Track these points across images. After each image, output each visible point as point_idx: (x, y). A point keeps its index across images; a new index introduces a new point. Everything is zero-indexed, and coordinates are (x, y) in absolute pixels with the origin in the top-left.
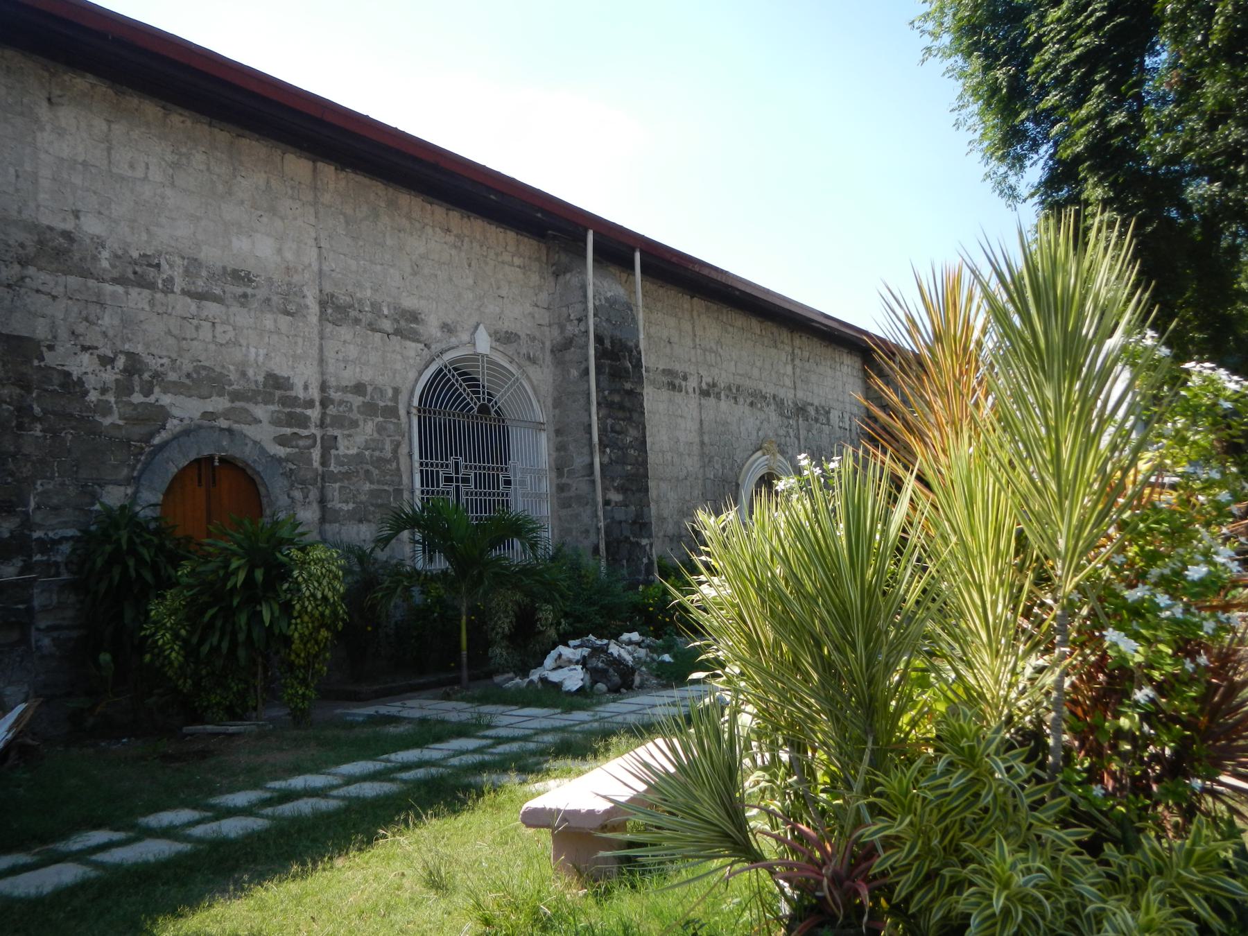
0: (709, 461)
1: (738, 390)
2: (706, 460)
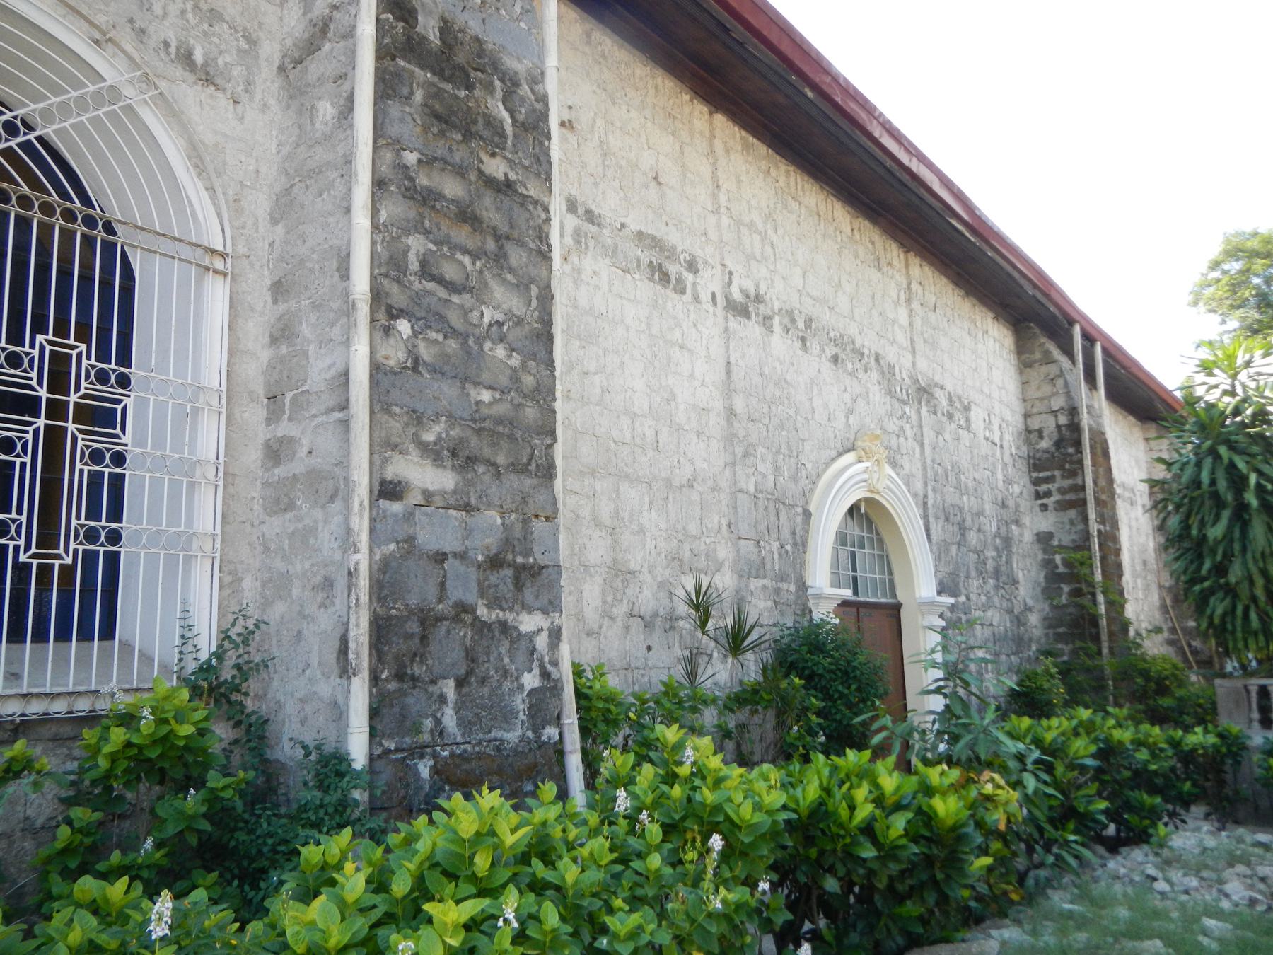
0: (746, 455)
1: (809, 322)
2: (739, 451)
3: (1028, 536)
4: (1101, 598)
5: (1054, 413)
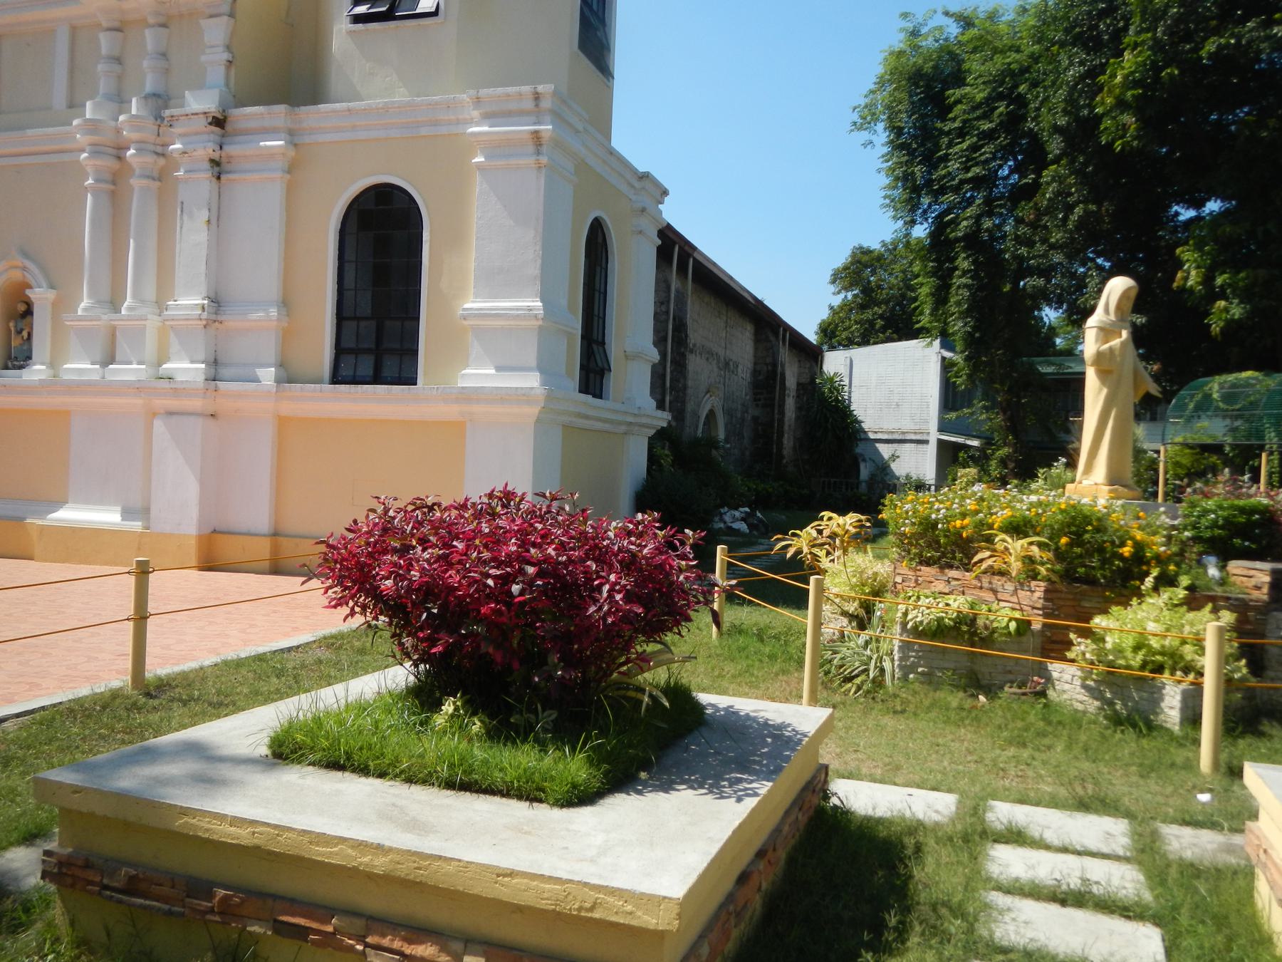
3: (749, 418)
5: (767, 365)
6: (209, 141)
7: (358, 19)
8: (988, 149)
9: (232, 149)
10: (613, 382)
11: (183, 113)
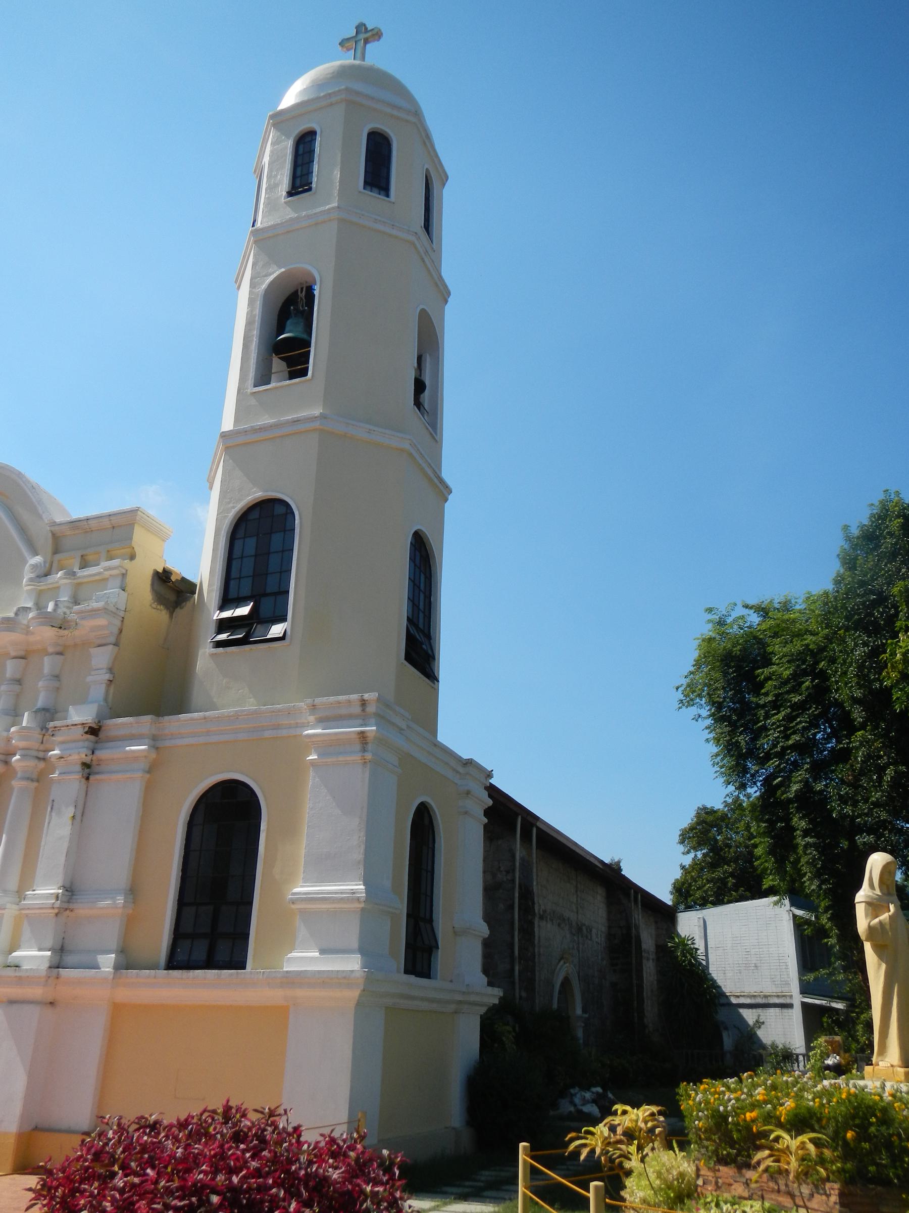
4: (636, 1015)
6: (84, 747)
7: (219, 644)
8: (802, 721)
9: (102, 754)
10: (441, 959)
11: (65, 724)
